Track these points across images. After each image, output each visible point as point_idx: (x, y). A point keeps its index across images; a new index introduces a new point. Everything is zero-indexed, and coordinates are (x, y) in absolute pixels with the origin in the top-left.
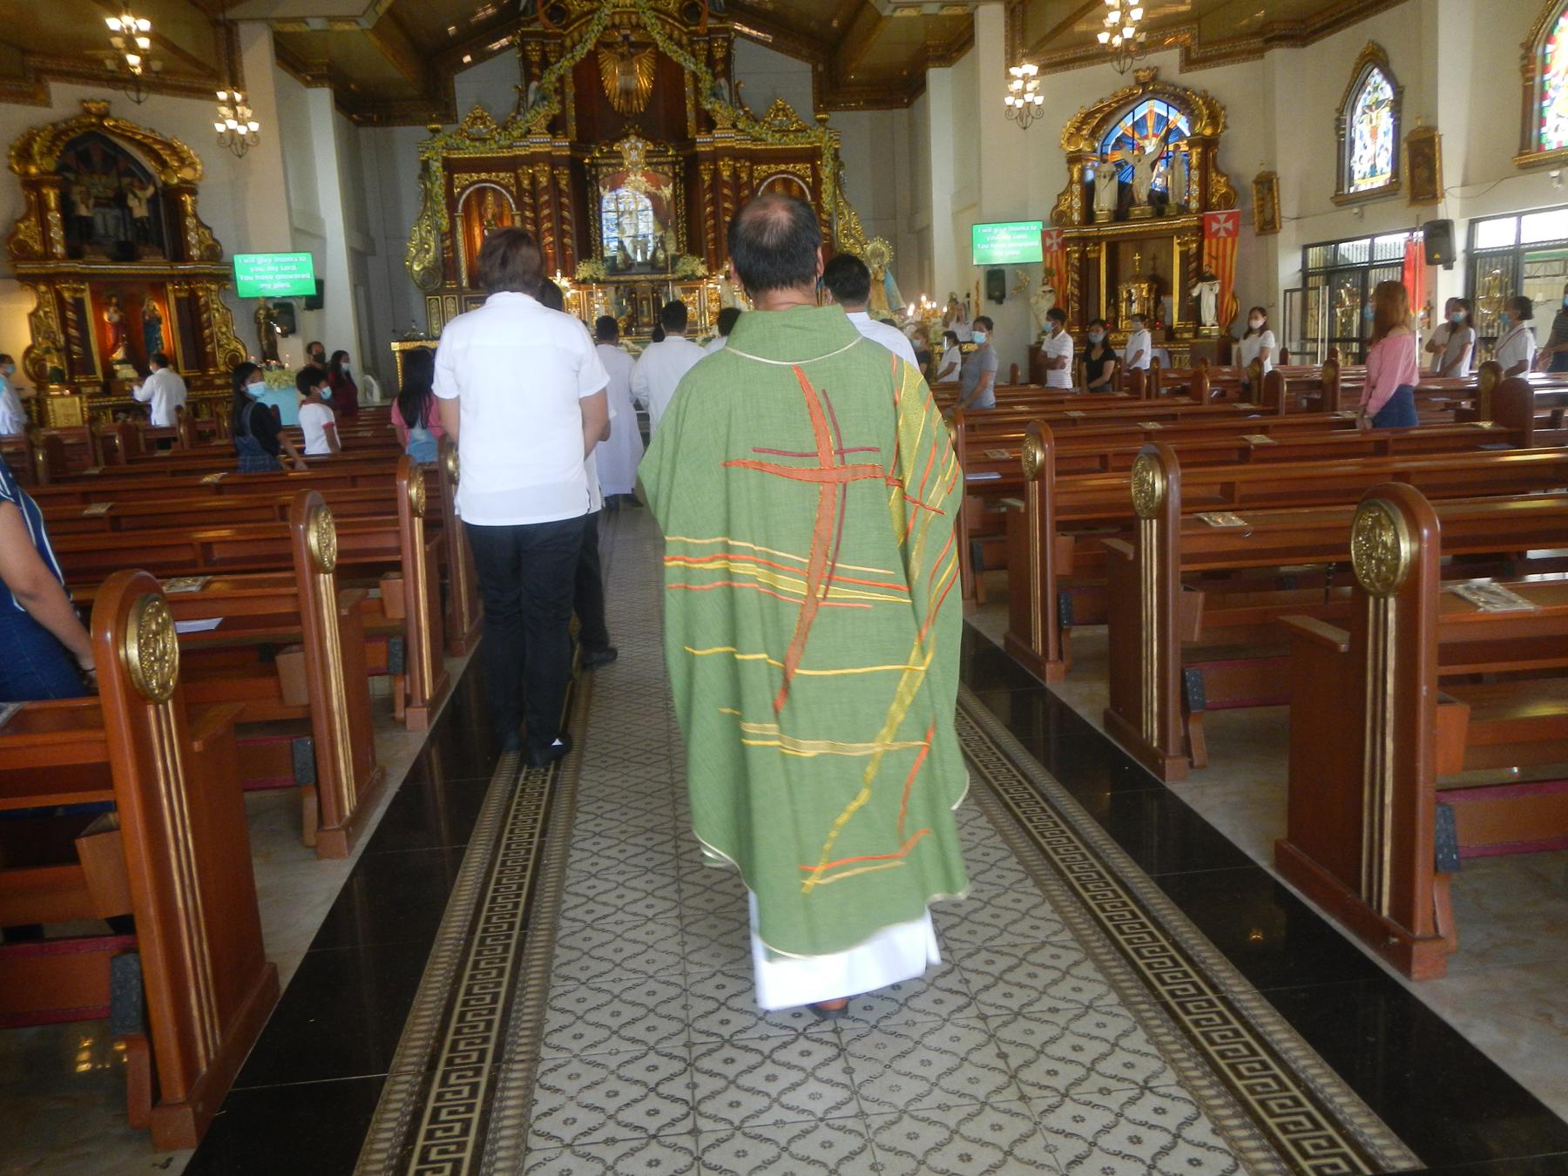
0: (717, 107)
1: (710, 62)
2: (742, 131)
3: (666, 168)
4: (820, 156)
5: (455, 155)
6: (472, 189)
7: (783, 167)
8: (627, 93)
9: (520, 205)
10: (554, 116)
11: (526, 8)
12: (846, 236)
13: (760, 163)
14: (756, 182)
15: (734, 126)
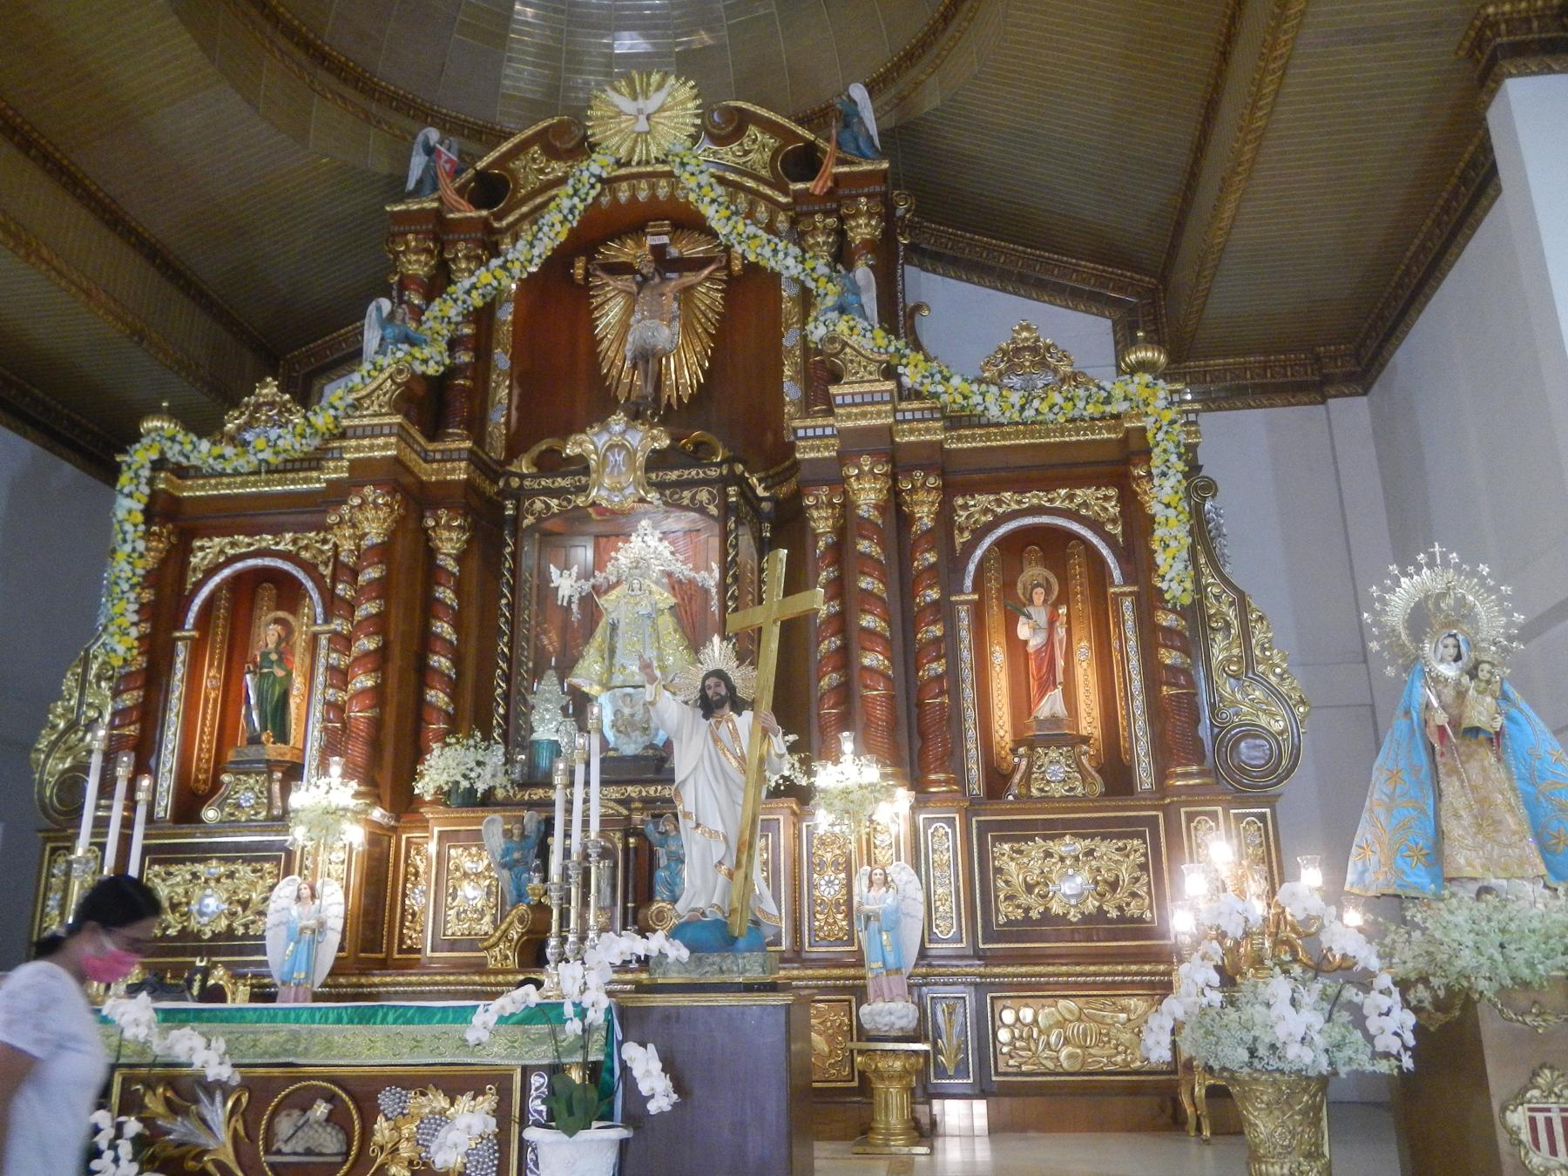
0: (842, 327)
1: (842, 256)
2: (905, 394)
3: (703, 496)
4: (1146, 453)
5: (192, 490)
6: (227, 572)
7: (1031, 499)
8: (647, 358)
9: (332, 604)
10: (424, 375)
11: (420, 182)
12: (1236, 677)
13: (970, 489)
14: (961, 539)
15: (890, 372)
